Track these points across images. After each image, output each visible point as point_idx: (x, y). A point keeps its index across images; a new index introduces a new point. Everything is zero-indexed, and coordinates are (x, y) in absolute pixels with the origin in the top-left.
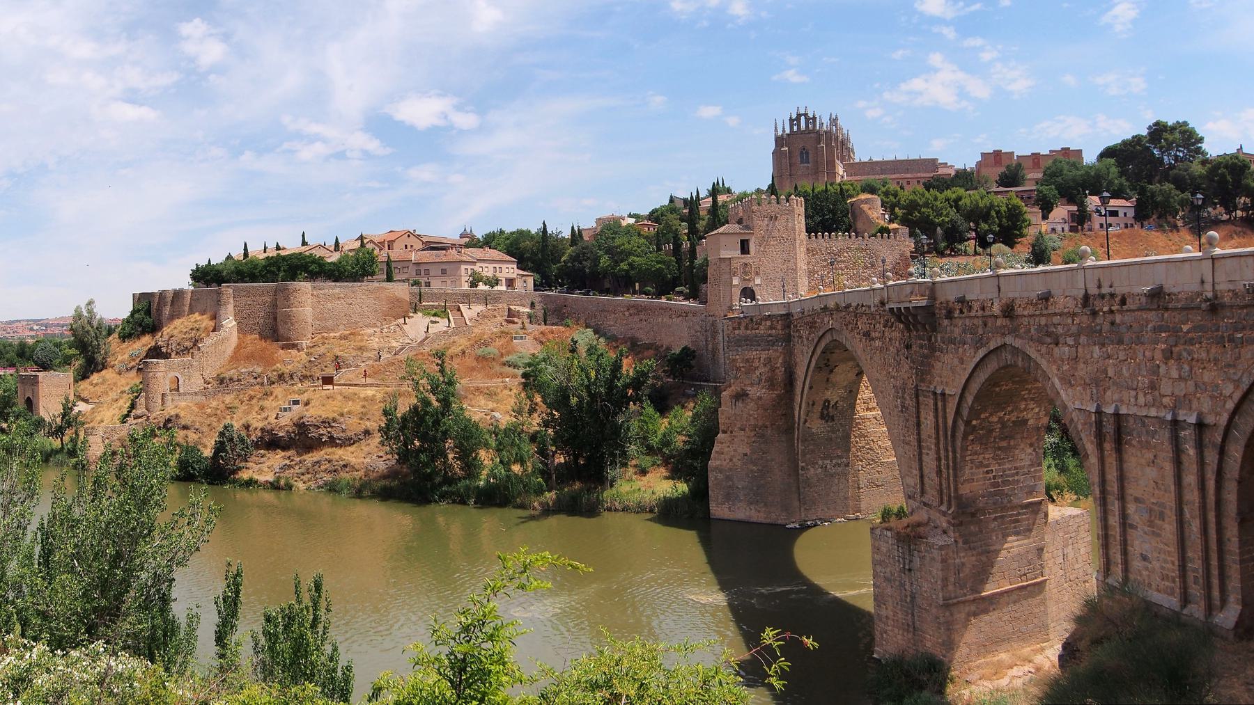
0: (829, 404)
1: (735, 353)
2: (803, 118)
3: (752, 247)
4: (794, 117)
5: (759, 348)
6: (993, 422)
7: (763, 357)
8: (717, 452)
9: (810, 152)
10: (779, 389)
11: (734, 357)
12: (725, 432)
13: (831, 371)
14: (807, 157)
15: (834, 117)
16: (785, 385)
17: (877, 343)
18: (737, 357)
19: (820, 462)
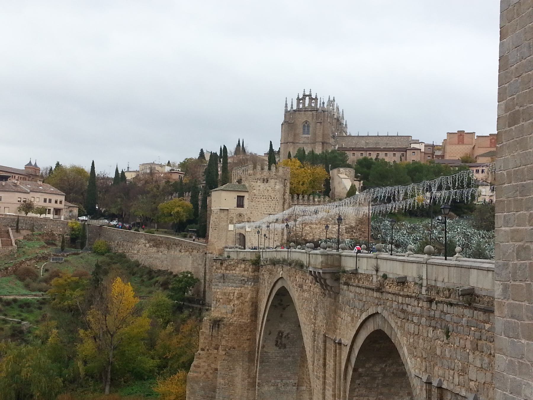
0: (282, 335)
1: (216, 287)
2: (307, 98)
3: (246, 202)
4: (301, 97)
5: (234, 285)
6: (376, 371)
7: (237, 292)
8: (195, 366)
9: (311, 126)
10: (247, 318)
11: (215, 290)
12: (203, 350)
13: (284, 309)
14: (308, 129)
15: (332, 99)
16: (251, 316)
17: (306, 295)
18: (218, 290)
19: (273, 381)
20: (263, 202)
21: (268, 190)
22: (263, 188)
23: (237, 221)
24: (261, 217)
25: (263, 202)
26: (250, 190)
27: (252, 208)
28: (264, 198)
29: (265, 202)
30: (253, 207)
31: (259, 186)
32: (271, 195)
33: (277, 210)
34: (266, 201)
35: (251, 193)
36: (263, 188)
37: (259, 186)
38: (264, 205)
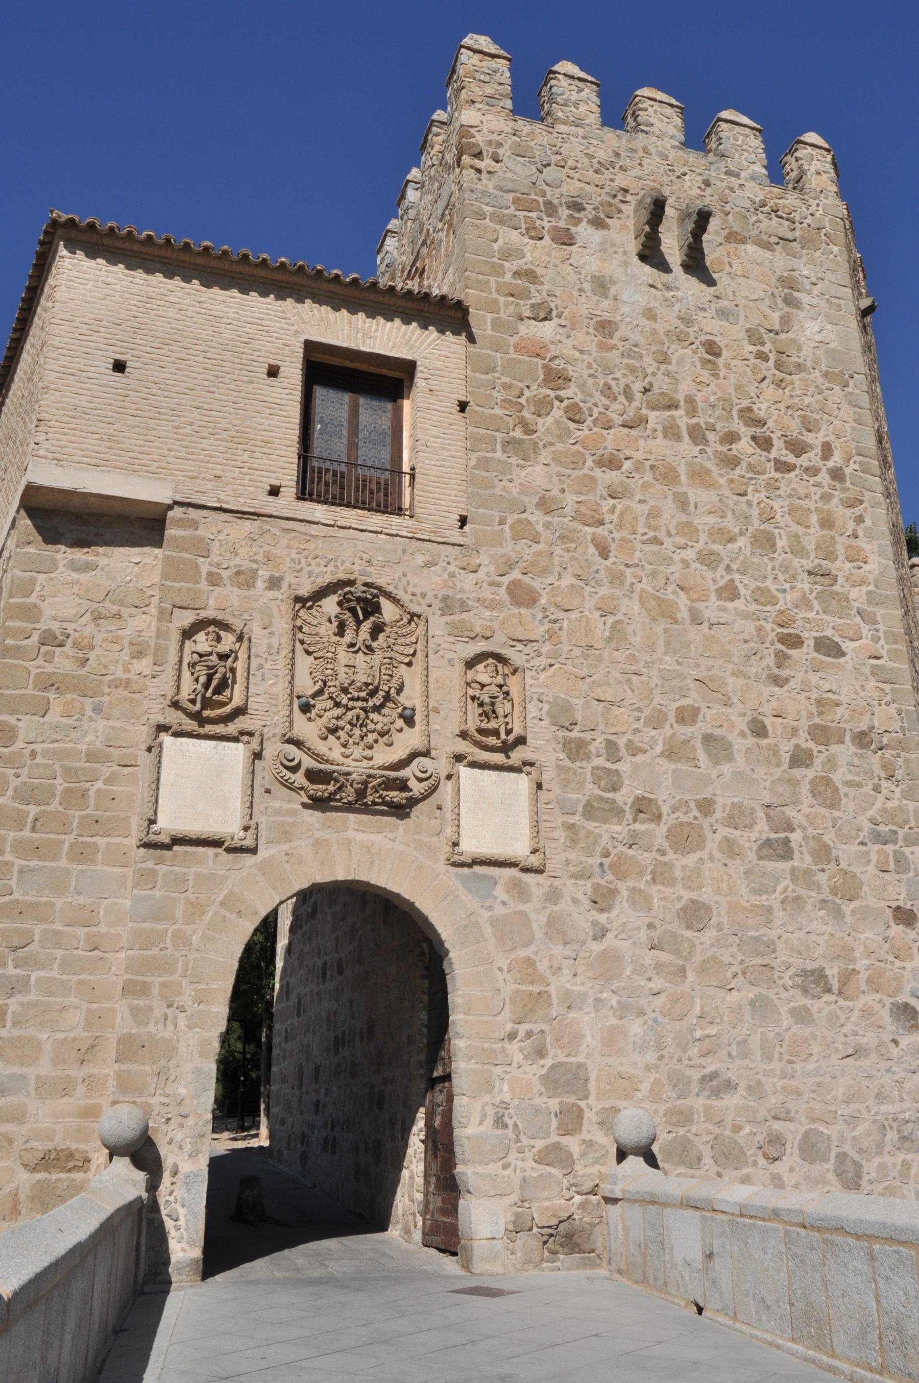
20: (668, 476)
21: (713, 349)
22: (650, 314)
23: (306, 685)
24: (668, 664)
25: (668, 476)
26: (493, 307)
27: (523, 532)
28: (671, 432)
29: (700, 476)
30: (537, 518)
31: (601, 285)
32: (761, 409)
33: (857, 595)
34: (710, 465)
35: (498, 347)
36: (650, 314)
37: (601, 285)
38: (683, 503)
